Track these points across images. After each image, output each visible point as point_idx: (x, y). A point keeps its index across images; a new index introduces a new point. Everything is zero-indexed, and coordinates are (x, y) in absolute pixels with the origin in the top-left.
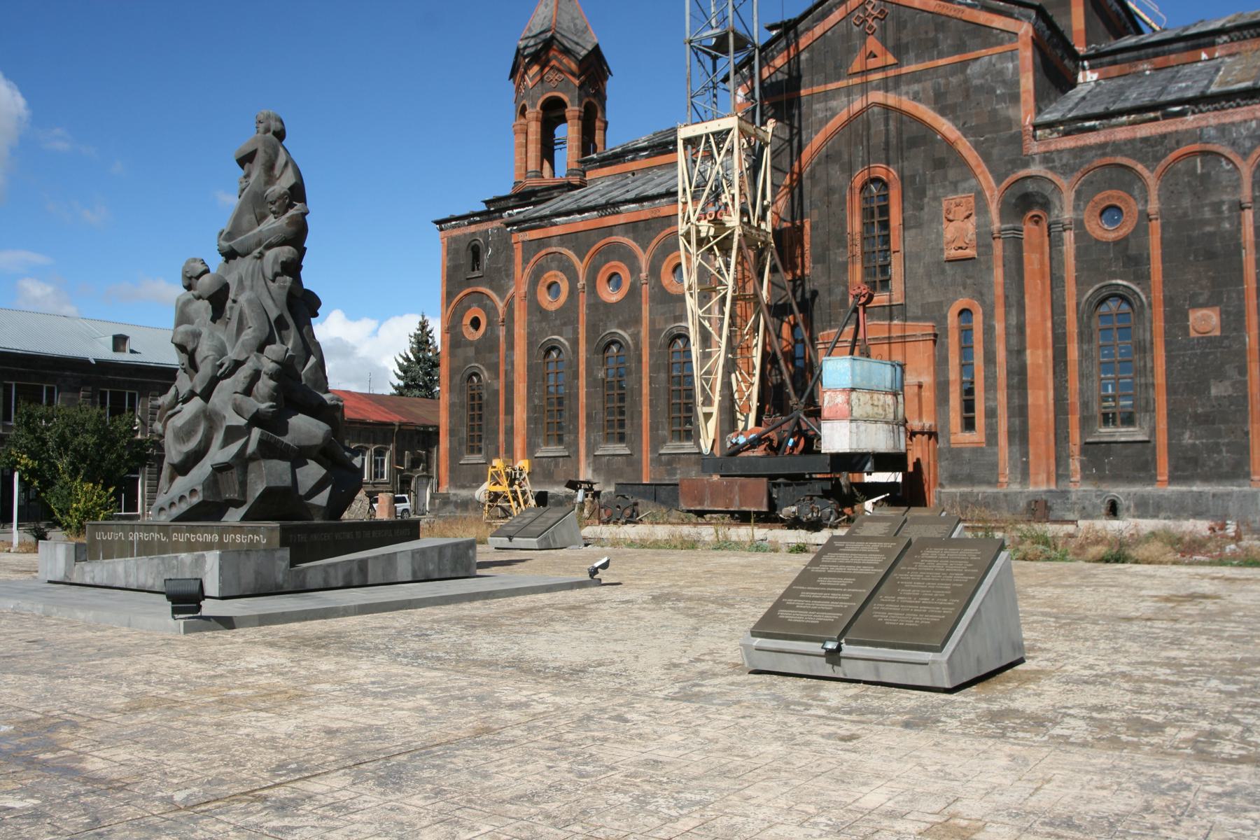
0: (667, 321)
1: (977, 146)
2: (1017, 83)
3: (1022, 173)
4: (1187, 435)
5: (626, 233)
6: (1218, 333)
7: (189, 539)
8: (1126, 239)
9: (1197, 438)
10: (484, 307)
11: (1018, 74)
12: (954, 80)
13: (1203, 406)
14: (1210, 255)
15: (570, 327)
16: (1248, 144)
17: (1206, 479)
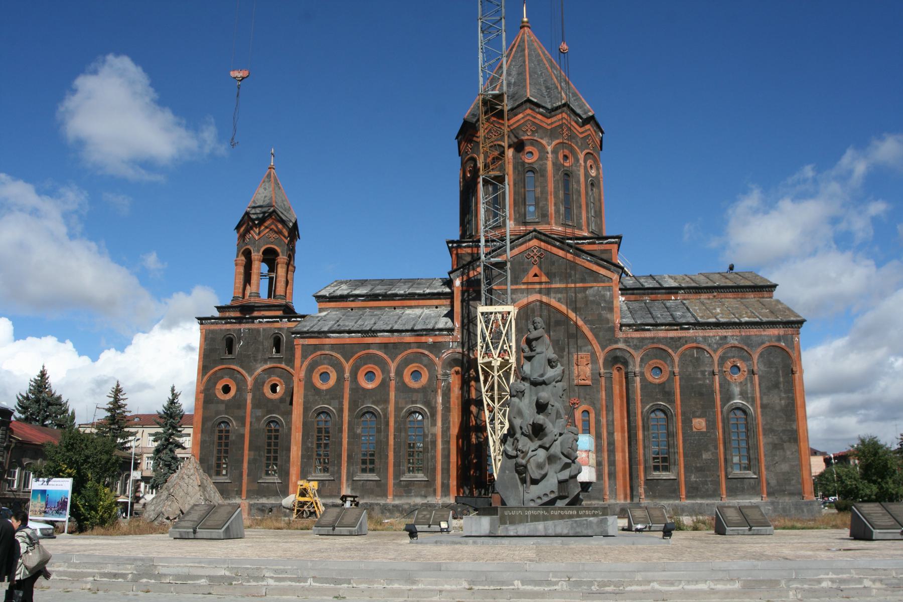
0: (407, 403)
1: (592, 330)
3: (615, 346)
5: (380, 349)
6: (705, 430)
10: (235, 379)
12: (580, 296)
14: (701, 394)
15: (337, 401)
16: (715, 346)
17: (702, 497)
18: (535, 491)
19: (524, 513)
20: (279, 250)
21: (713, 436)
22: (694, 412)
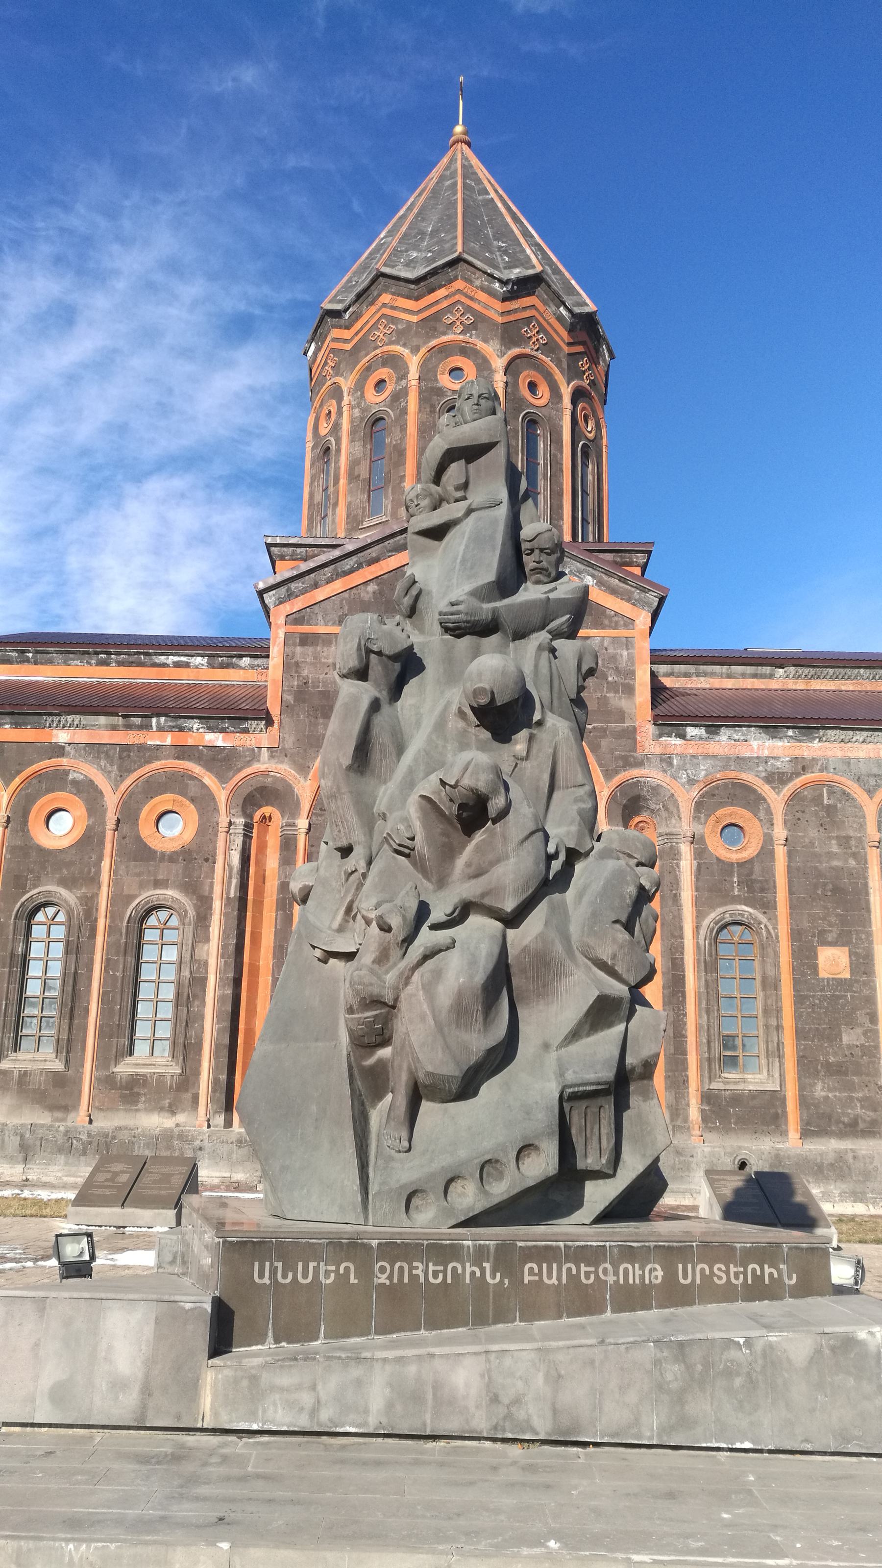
0: (142, 886)
4: (819, 1086)
6: (847, 975)
7: (574, 1279)
8: (751, 861)
9: (830, 1090)
11: (633, 664)
13: (835, 1054)
14: (837, 890)
16: (872, 782)
19: (366, 1273)
21: (866, 992)
22: (822, 933)
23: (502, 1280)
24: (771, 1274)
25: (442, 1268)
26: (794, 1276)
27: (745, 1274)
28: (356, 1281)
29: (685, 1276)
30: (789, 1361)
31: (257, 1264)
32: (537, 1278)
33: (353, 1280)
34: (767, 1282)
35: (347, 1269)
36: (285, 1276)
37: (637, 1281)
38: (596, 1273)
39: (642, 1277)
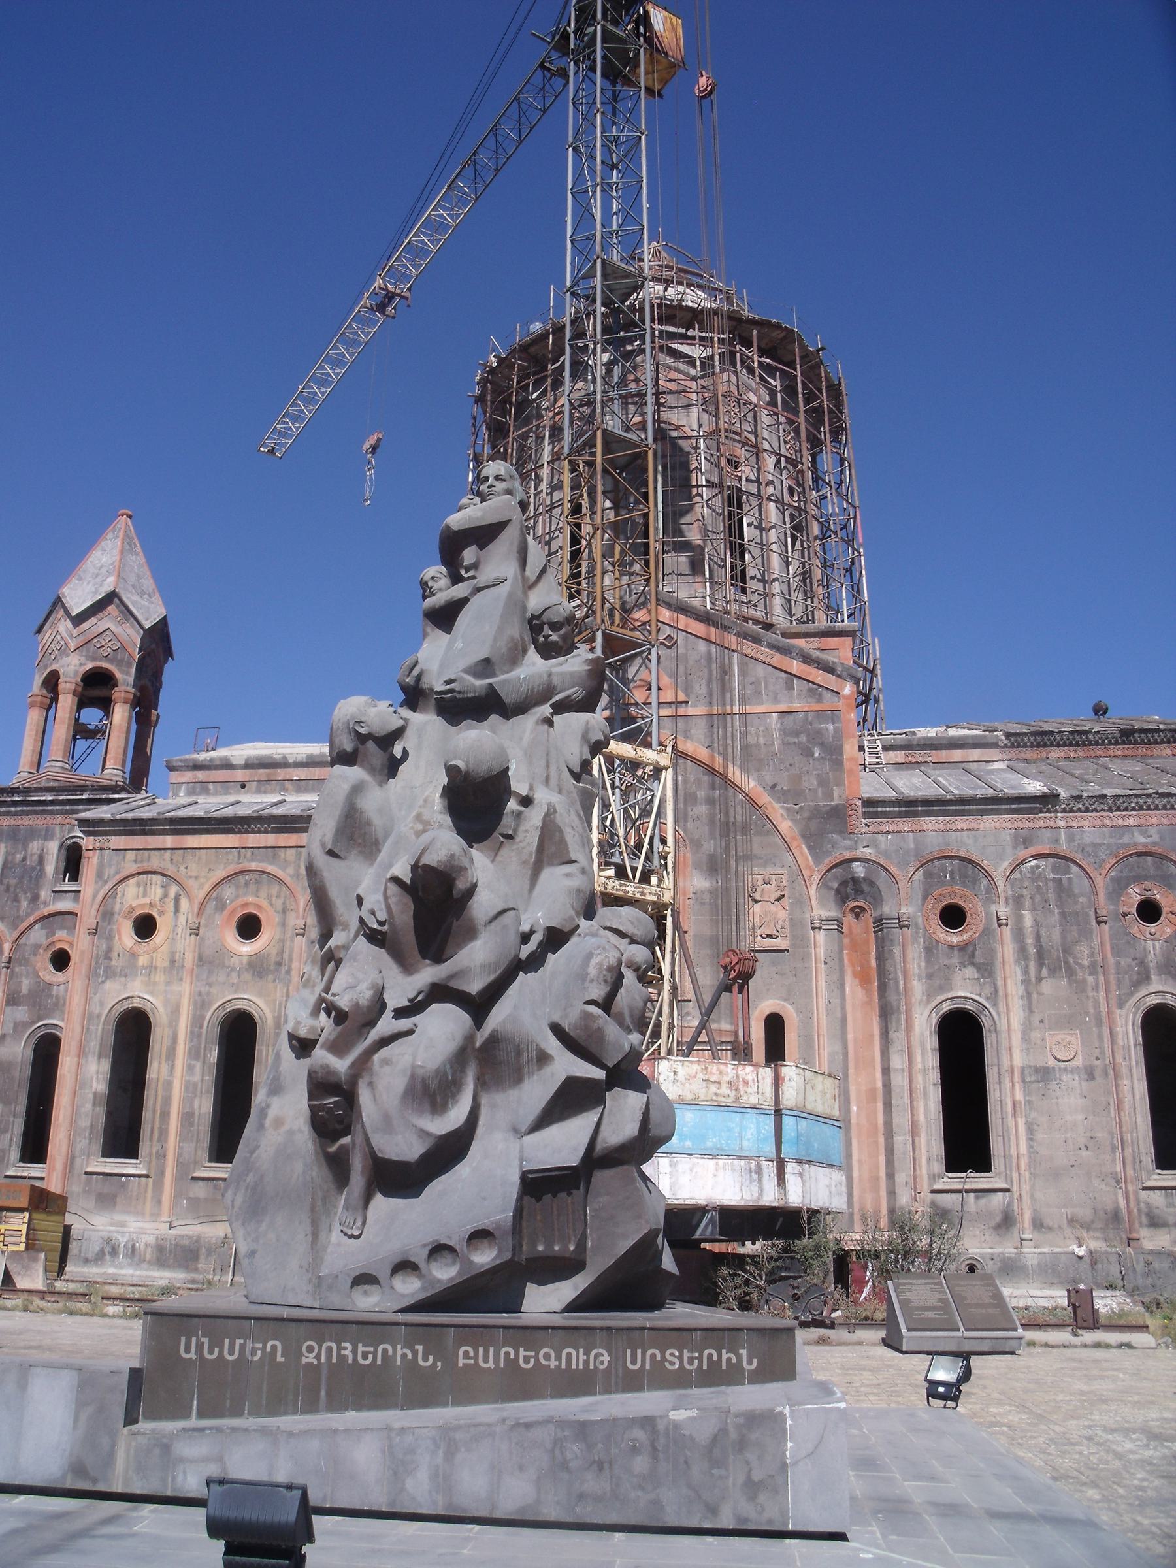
2: (839, 750)
7: (512, 1364)
18: (397, 1223)
19: (293, 1352)
20: (118, 675)
23: (434, 1364)
24: (729, 1359)
25: (371, 1349)
26: (755, 1361)
27: (700, 1359)
28: (283, 1359)
29: (634, 1362)
30: (692, 1438)
31: (183, 1339)
32: (472, 1361)
33: (280, 1358)
34: (724, 1367)
35: (274, 1347)
36: (211, 1352)
37: (581, 1366)
38: (536, 1358)
39: (586, 1362)
